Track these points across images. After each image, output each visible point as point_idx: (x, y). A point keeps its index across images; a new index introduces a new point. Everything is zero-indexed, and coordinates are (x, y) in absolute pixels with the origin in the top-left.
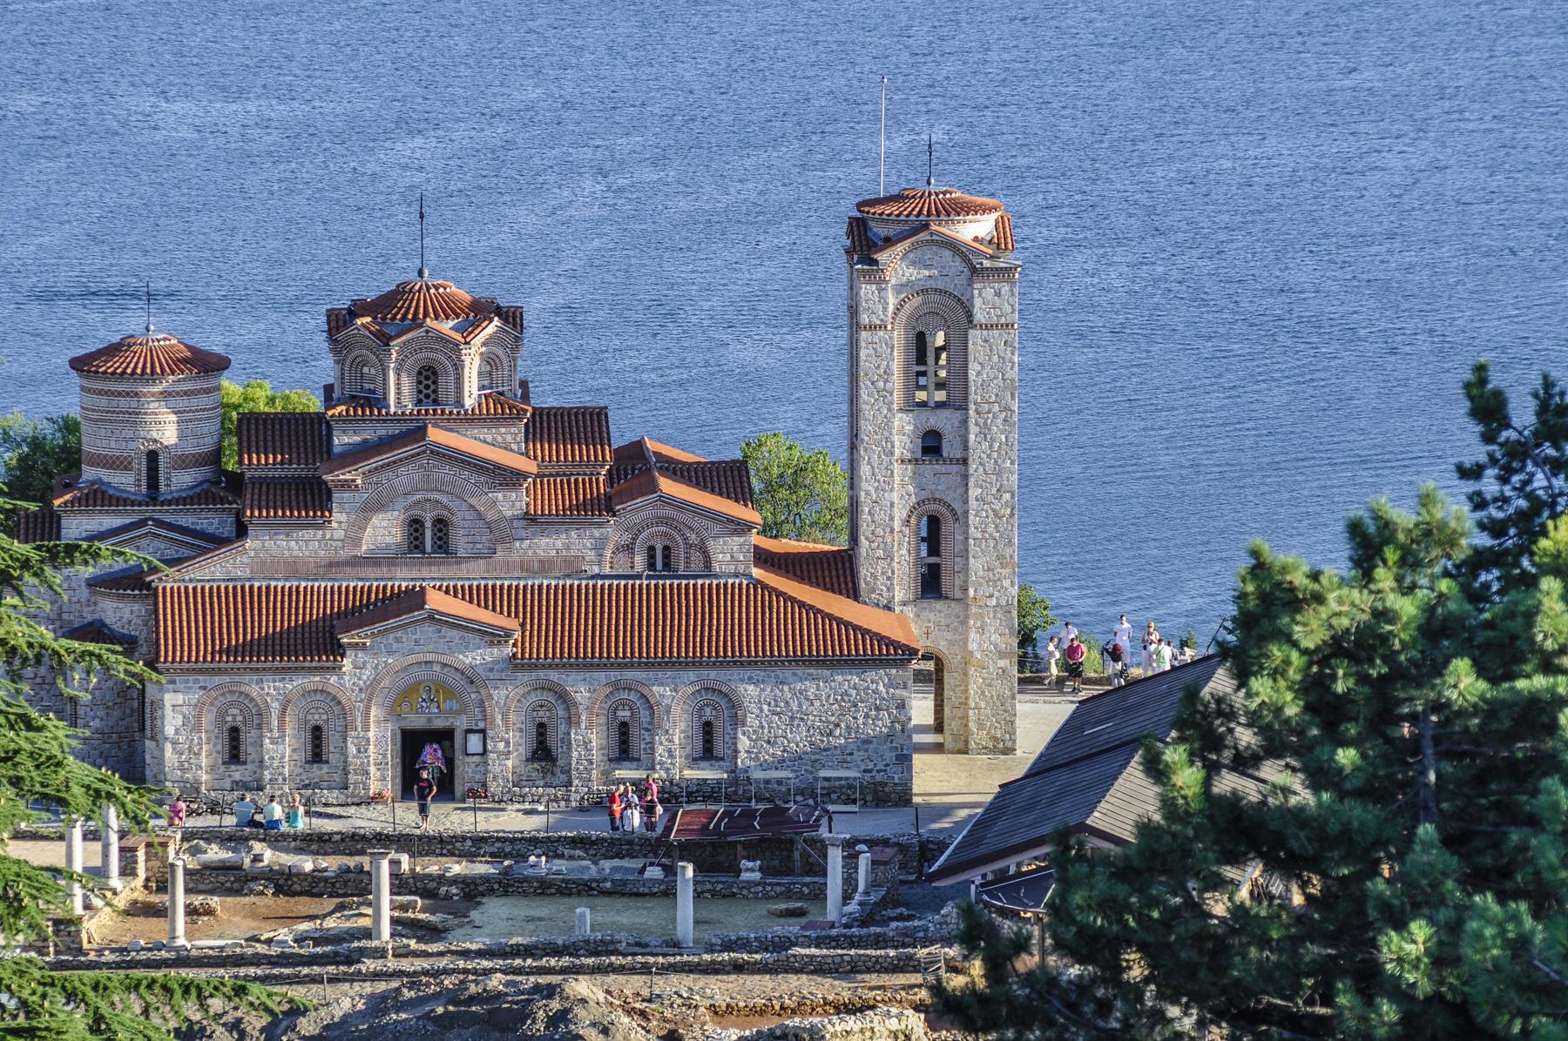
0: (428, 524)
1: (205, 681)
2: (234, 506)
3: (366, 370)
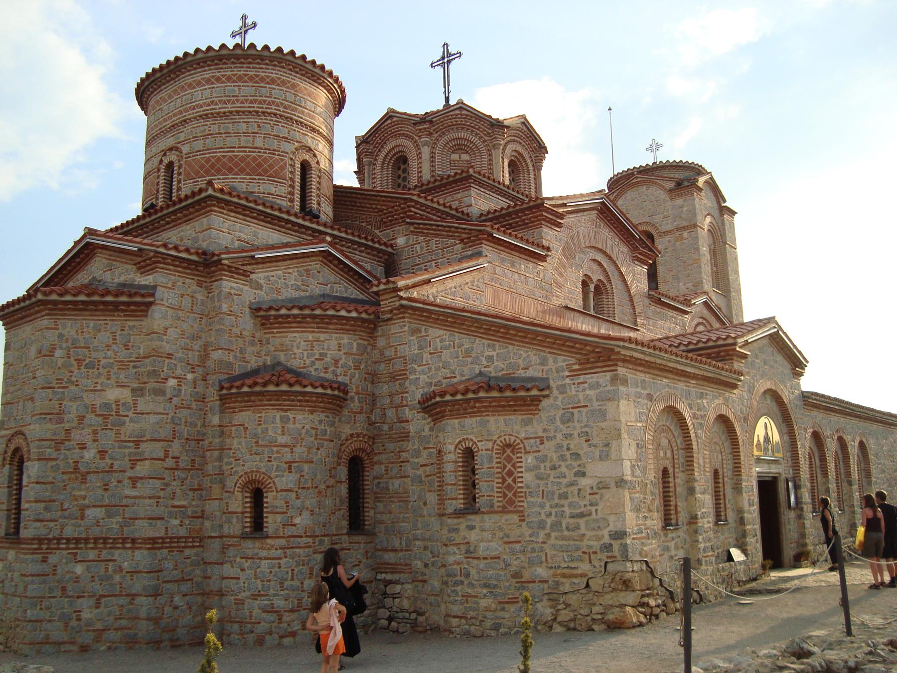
3: (455, 157)
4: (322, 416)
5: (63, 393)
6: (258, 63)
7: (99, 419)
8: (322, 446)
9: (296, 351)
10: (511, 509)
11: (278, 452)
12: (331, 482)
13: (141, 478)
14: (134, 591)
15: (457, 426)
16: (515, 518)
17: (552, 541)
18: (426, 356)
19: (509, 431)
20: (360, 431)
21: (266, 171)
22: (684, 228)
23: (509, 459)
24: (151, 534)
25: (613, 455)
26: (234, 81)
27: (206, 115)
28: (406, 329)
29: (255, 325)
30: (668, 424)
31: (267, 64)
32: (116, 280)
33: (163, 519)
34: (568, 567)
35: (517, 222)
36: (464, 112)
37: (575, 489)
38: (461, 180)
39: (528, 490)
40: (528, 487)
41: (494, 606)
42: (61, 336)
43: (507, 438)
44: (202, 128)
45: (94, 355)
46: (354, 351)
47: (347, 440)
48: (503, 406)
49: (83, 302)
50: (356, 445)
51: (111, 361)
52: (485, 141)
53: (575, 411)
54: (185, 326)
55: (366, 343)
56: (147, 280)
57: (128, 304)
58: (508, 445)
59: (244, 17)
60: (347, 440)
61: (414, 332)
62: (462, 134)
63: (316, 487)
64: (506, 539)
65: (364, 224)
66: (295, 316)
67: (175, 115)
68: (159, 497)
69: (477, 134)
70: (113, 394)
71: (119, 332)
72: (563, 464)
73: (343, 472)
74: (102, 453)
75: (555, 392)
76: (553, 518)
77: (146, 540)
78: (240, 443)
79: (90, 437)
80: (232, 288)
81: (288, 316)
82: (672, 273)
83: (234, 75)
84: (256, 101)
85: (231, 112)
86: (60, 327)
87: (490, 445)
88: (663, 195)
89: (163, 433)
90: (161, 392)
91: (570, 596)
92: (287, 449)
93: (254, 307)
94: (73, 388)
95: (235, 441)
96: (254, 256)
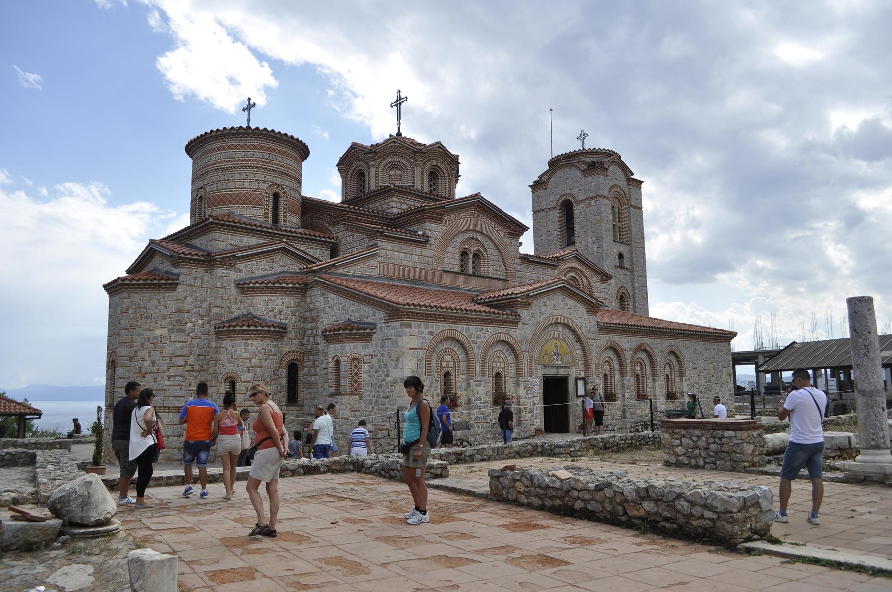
0: (471, 256)
1: (432, 328)
2: (332, 241)
3: (392, 173)
4: (269, 342)
5: (133, 332)
6: (246, 137)
7: (152, 345)
8: (269, 359)
9: (259, 306)
10: (357, 393)
11: (242, 362)
12: (274, 377)
13: (173, 376)
14: (169, 434)
15: (333, 348)
16: (357, 397)
17: (375, 410)
18: (327, 309)
19: (356, 351)
20: (294, 349)
21: (250, 202)
22: (592, 198)
23: (356, 366)
24: (177, 404)
25: (400, 366)
26: (233, 149)
27: (218, 169)
28: (319, 293)
29: (237, 292)
30: (452, 347)
31: (251, 137)
32: (164, 269)
33: (184, 397)
34: (380, 425)
35: (413, 220)
36: (397, 144)
37: (384, 383)
38: (387, 191)
39: (364, 383)
40: (364, 381)
41: (345, 444)
42: (132, 302)
43: (355, 355)
44: (216, 177)
45: (149, 311)
46: (293, 305)
47: (287, 354)
48: (353, 338)
49: (142, 284)
50: (293, 357)
51: (158, 314)
52: (410, 162)
53: (386, 341)
54: (197, 295)
55: (300, 300)
56: (176, 271)
57: (166, 284)
58: (356, 359)
59: (249, 99)
60: (287, 354)
61: (323, 294)
62: (396, 159)
63: (264, 380)
64: (352, 409)
65: (324, 223)
66: (258, 288)
67: (203, 168)
68: (182, 386)
69: (405, 158)
70: (159, 332)
71: (162, 299)
72: (380, 370)
73: (284, 372)
74: (153, 363)
75: (378, 331)
76: (375, 398)
77: (175, 408)
78: (224, 357)
79: (147, 355)
80: (223, 273)
81: (254, 287)
82: (583, 230)
83: (233, 145)
84: (245, 160)
85: (231, 167)
86: (131, 297)
87: (346, 359)
88: (579, 174)
89: (184, 352)
90: (183, 331)
91: (381, 440)
92: (248, 361)
93: (237, 283)
94: (138, 329)
95: (222, 356)
96: (235, 255)
